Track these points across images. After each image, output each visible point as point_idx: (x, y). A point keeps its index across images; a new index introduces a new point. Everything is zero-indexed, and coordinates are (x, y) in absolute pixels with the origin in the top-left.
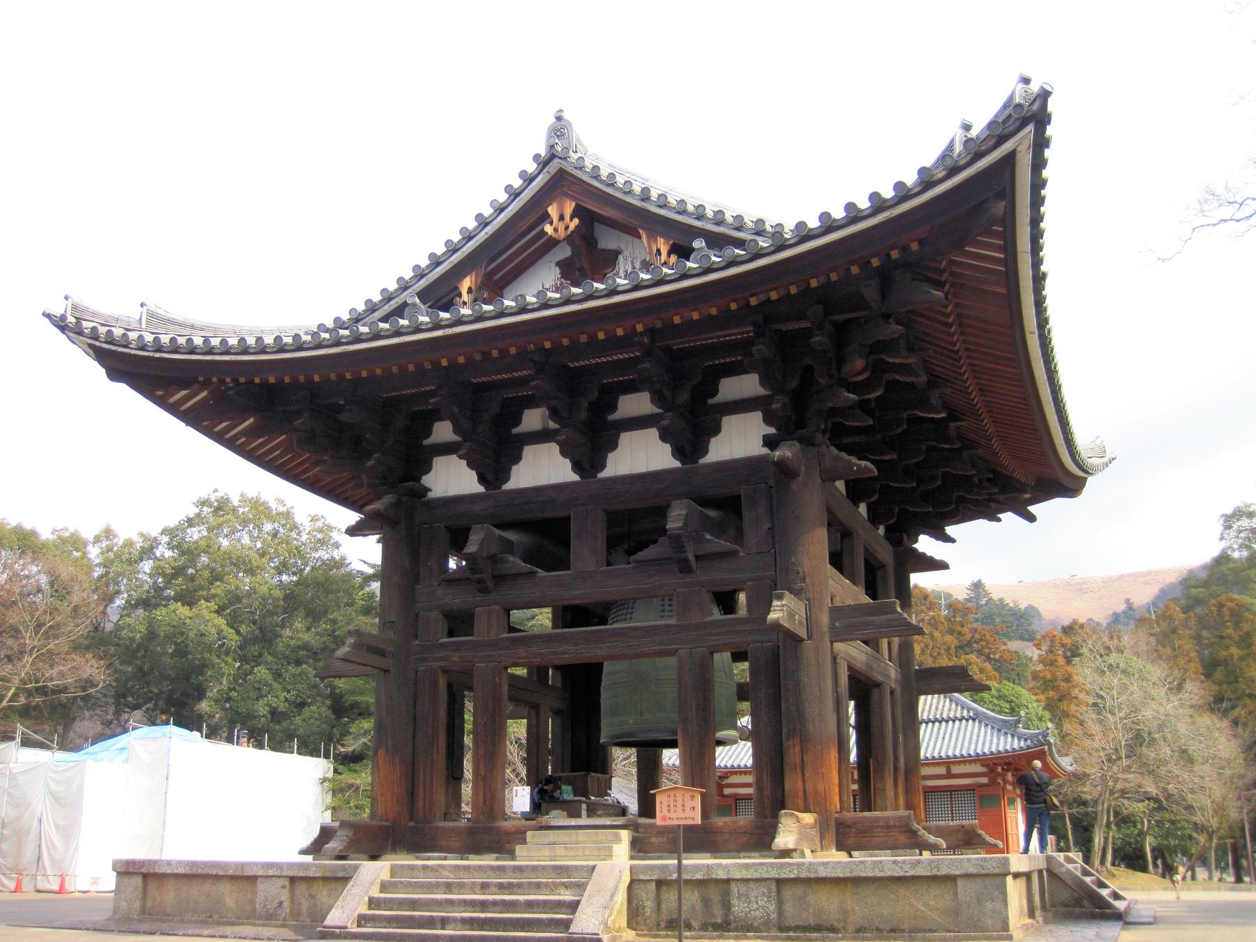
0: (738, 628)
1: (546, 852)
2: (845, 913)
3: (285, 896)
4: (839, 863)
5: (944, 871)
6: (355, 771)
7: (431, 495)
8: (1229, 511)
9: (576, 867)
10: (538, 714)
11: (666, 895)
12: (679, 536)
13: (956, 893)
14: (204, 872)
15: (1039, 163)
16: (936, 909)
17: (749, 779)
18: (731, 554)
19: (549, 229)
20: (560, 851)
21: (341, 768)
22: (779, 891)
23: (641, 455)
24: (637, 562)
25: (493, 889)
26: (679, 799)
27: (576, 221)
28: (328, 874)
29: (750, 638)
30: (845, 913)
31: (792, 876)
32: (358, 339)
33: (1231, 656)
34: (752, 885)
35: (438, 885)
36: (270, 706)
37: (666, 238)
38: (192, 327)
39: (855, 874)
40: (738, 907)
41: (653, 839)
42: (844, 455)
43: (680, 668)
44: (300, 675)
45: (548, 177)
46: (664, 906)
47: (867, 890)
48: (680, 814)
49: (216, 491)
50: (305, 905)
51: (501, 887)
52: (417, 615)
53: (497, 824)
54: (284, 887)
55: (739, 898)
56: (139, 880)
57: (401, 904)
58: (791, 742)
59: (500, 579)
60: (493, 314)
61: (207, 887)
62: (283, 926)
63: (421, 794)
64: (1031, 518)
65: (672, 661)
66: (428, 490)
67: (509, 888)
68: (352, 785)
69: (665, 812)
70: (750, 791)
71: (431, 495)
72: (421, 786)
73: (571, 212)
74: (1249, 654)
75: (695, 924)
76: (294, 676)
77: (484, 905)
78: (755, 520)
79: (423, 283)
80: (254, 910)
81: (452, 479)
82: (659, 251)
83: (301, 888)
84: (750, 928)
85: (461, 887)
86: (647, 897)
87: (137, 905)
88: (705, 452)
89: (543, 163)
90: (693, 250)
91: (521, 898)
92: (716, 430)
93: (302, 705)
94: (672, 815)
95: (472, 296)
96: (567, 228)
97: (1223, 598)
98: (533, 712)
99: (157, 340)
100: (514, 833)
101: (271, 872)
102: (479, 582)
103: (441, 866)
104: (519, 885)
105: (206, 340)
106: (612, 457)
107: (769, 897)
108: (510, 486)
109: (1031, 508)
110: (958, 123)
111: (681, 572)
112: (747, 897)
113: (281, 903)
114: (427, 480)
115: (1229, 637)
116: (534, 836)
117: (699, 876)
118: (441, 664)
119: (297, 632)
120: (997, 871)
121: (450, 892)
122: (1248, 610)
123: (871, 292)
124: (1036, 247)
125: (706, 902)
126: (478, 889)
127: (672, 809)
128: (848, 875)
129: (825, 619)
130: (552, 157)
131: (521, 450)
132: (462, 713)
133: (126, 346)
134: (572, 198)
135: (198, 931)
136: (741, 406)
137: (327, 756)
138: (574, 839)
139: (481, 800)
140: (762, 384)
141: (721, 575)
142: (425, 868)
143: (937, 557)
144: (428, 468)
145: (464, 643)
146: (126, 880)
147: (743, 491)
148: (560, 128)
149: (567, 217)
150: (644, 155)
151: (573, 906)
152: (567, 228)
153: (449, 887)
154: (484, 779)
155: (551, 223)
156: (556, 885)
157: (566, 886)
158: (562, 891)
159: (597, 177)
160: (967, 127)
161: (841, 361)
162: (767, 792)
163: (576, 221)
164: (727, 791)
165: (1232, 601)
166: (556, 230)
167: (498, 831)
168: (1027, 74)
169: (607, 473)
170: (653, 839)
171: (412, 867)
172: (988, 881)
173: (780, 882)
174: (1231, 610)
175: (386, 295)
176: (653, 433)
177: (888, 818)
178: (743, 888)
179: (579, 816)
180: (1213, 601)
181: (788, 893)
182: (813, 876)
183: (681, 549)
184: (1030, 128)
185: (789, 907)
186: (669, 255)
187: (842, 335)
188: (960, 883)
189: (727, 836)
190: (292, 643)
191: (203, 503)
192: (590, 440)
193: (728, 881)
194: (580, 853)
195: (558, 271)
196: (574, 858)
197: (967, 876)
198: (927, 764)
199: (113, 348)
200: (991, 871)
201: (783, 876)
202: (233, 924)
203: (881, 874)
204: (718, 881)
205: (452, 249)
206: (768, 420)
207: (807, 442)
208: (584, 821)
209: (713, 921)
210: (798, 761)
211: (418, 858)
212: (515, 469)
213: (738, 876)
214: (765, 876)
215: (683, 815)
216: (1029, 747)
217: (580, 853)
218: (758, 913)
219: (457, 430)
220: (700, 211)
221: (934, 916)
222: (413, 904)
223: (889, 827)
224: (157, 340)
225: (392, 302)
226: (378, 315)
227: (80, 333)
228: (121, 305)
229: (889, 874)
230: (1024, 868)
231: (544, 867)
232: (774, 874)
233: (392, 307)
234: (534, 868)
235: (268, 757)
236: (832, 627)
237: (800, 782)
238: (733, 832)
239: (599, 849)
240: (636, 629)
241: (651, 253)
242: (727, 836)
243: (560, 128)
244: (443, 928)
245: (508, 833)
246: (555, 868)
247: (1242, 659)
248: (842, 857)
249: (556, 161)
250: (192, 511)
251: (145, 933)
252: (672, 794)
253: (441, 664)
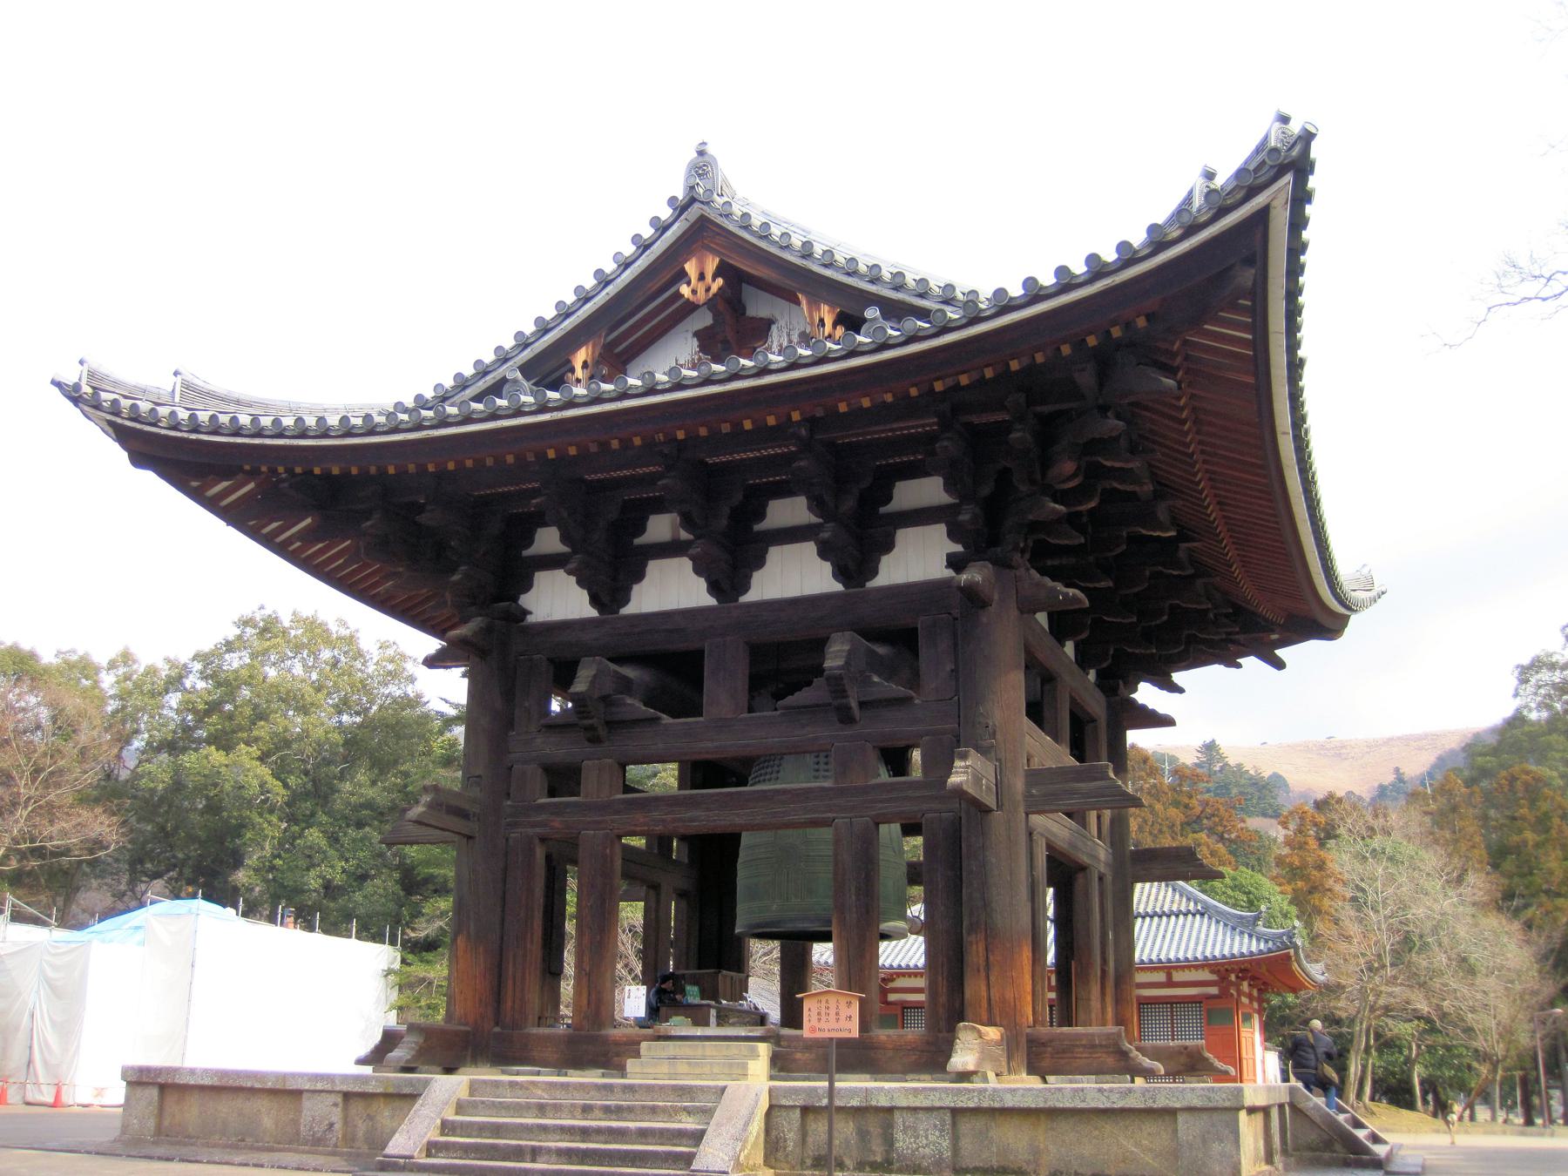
0: (910, 793)
1: (664, 1068)
2: (1036, 1152)
3: (336, 1116)
4: (1030, 1090)
5: (1161, 1103)
6: (428, 962)
7: (531, 619)
8: (1526, 661)
9: (702, 1088)
10: (658, 894)
11: (814, 1126)
12: (839, 678)
13: (1175, 1131)
14: (237, 1084)
15: (1298, 222)
16: (1150, 1150)
17: (920, 983)
18: (904, 701)
19: (685, 290)
20: (682, 1067)
21: (410, 957)
22: (954, 1124)
23: (795, 575)
24: (786, 708)
25: (601, 1115)
26: (833, 1004)
27: (720, 281)
28: (391, 1090)
29: (925, 807)
30: (1036, 1152)
31: (971, 1105)
32: (444, 422)
33: (1525, 842)
34: (921, 1115)
35: (528, 1107)
36: (324, 878)
37: (832, 305)
38: (238, 402)
39: (1050, 1104)
40: (903, 1142)
41: (798, 1056)
42: (1047, 581)
43: (837, 842)
44: (362, 840)
45: (686, 225)
46: (810, 1140)
47: (1064, 1125)
48: (833, 1024)
49: (262, 608)
50: (362, 1128)
51: (607, 1110)
52: (510, 769)
53: (603, 1032)
54: (335, 1105)
55: (905, 1131)
56: (155, 1092)
57: (482, 1129)
58: (972, 938)
59: (613, 725)
60: (613, 395)
61: (239, 1102)
62: (333, 1154)
63: (510, 992)
64: (1279, 664)
65: (826, 833)
66: (526, 613)
67: (617, 1112)
68: (424, 980)
69: (814, 1022)
70: (921, 997)
71: (531, 619)
72: (510, 982)
73: (714, 271)
74: (1547, 840)
75: (848, 1162)
76: (354, 840)
77: (585, 1133)
78: (934, 659)
79: (527, 354)
80: (298, 1133)
81: (557, 599)
82: (822, 321)
83: (357, 1107)
85: (557, 1109)
86: (790, 1127)
87: (151, 1124)
88: (875, 573)
89: (680, 208)
90: (865, 320)
91: (632, 1125)
92: (888, 546)
93: (364, 877)
94: (823, 1025)
95: (587, 372)
96: (708, 289)
97: (1517, 768)
98: (652, 892)
99: (193, 417)
100: (626, 1044)
101: (319, 1086)
102: (586, 729)
103: (533, 1083)
104: (630, 1109)
105: (255, 419)
106: (757, 577)
107: (941, 1131)
108: (628, 610)
109: (1279, 652)
110: (1199, 171)
111: (841, 722)
112: (915, 1129)
113: (331, 1125)
114: (526, 600)
115: (1523, 818)
116: (649, 1048)
117: (855, 1103)
118: (538, 830)
119: (360, 786)
120: (1227, 1104)
121: (544, 1116)
122: (1548, 785)
123: (1086, 379)
124: (1292, 326)
125: (863, 1135)
126: (578, 1113)
127: (824, 1018)
128: (1041, 1105)
129: (1019, 784)
130: (692, 200)
131: (645, 566)
132: (563, 892)
133: (154, 425)
134: (715, 252)
135: (226, 1158)
136: (920, 517)
137: (393, 943)
138: (700, 1052)
139: (585, 1002)
140: (947, 489)
141: (891, 726)
142: (512, 1084)
143: (1161, 710)
144: (527, 586)
145: (567, 804)
146: (139, 1091)
147: (921, 623)
148: (702, 165)
149: (709, 277)
150: (808, 200)
151: (697, 1137)
152: (708, 289)
153: (541, 1109)
154: (589, 975)
155: (689, 283)
156: (676, 1110)
157: (688, 1111)
158: (684, 1117)
159: (747, 228)
160: (1210, 176)
161: (1046, 463)
162: (943, 999)
163: (720, 281)
164: (892, 997)
165: (1527, 773)
166: (694, 292)
167: (605, 1041)
168: (1286, 111)
169: (751, 596)
170: (798, 1056)
171: (497, 1084)
172: (1216, 1116)
173: (956, 1112)
174: (1526, 784)
175: (481, 368)
176: (810, 548)
177: (1093, 1035)
178: (910, 1119)
179: (707, 1024)
180: (1504, 773)
181: (966, 1126)
182: (997, 1105)
183: (843, 693)
184: (1289, 178)
185: (966, 1144)
186: (834, 327)
187: (1048, 431)
188: (1181, 1118)
189: (890, 1053)
190: (353, 799)
191: (246, 622)
192: (731, 556)
193: (890, 1110)
194: (707, 1070)
195: (694, 344)
196: (699, 1076)
197: (1190, 1109)
198: (1142, 969)
199: (138, 426)
200: (1221, 1104)
201: (960, 1105)
202: (271, 1150)
203: (1083, 1105)
204: (878, 1110)
205: (565, 313)
206: (953, 535)
207: (1002, 564)
208: (712, 1030)
209: (872, 1158)
210: (982, 962)
211: (504, 1072)
212: (636, 588)
213: (904, 1104)
214: (938, 1104)
215: (836, 1026)
216: (1270, 951)
217: (707, 1070)
218: (927, 1150)
219: (565, 538)
220: (875, 272)
221: (1148, 1159)
222: (497, 1130)
223: (1093, 1046)
224: (193, 417)
225: (488, 378)
226: (469, 392)
227: (98, 407)
228: (150, 372)
229: (1093, 1105)
230: (1260, 1101)
231: (662, 1087)
232: (948, 1102)
233: (488, 383)
234: (649, 1088)
235: (318, 941)
236: (1028, 796)
237: (984, 988)
238: (897, 1049)
239: (731, 1065)
240: (784, 792)
241: (812, 324)
242: (890, 1053)
243: (702, 165)
244: (533, 1161)
245: (617, 1043)
246: (675, 1088)
247: (1537, 845)
248: (1034, 1082)
249: (696, 205)
250: (232, 632)
251: (160, 1159)
252: (823, 999)
253: (538, 830)
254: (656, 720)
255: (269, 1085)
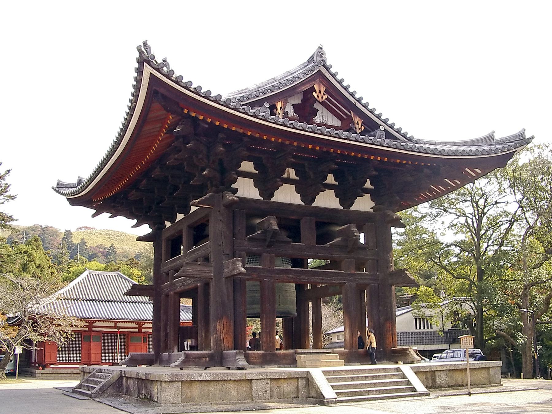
17: (151, 325)
19: (314, 94)
27: (325, 97)
29: (371, 282)
34: (442, 372)
50: (275, 391)
54: (267, 384)
61: (220, 386)
70: (151, 331)
73: (316, 89)
82: (358, 123)
83: (274, 383)
84: (441, 387)
101: (261, 377)
148: (320, 52)
149: (322, 92)
152: (322, 97)
176: (332, 192)
186: (361, 126)
192: (308, 190)
254: (289, 243)
255: (238, 378)
